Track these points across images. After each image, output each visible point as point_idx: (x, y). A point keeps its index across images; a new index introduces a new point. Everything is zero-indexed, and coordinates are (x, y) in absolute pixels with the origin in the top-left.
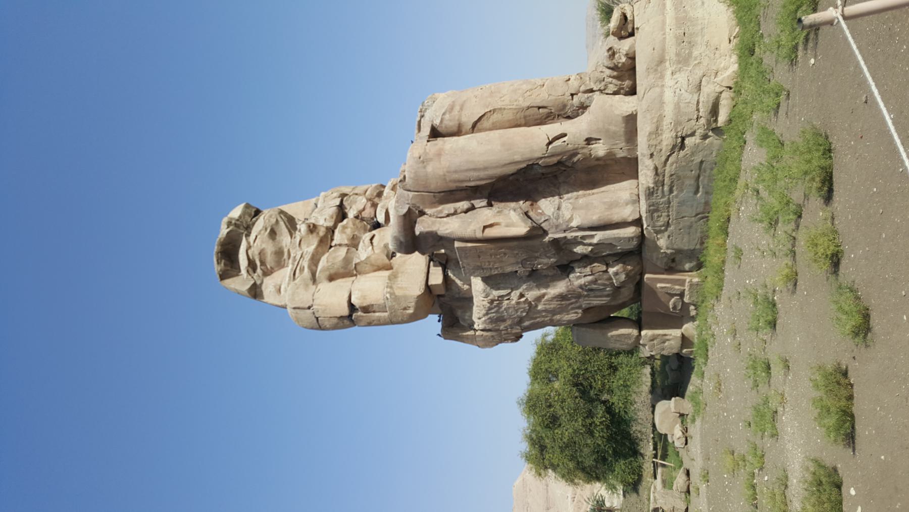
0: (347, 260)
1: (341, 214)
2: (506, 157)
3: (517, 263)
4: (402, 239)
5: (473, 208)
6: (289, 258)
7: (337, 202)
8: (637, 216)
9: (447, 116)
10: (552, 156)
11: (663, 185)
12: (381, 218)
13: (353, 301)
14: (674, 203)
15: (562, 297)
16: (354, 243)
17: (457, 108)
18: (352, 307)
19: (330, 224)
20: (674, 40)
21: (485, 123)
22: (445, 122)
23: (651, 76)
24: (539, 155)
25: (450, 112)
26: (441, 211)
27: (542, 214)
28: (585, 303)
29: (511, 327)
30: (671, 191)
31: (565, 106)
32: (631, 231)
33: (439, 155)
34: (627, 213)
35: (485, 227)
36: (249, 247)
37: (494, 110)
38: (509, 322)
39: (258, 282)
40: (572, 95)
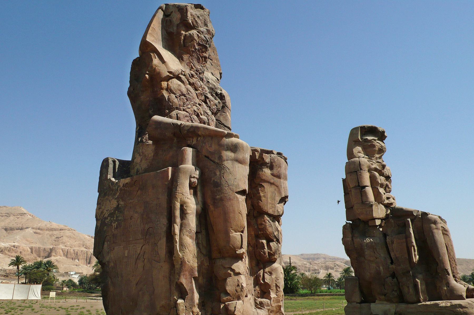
2: (441, 254)
16: (382, 186)
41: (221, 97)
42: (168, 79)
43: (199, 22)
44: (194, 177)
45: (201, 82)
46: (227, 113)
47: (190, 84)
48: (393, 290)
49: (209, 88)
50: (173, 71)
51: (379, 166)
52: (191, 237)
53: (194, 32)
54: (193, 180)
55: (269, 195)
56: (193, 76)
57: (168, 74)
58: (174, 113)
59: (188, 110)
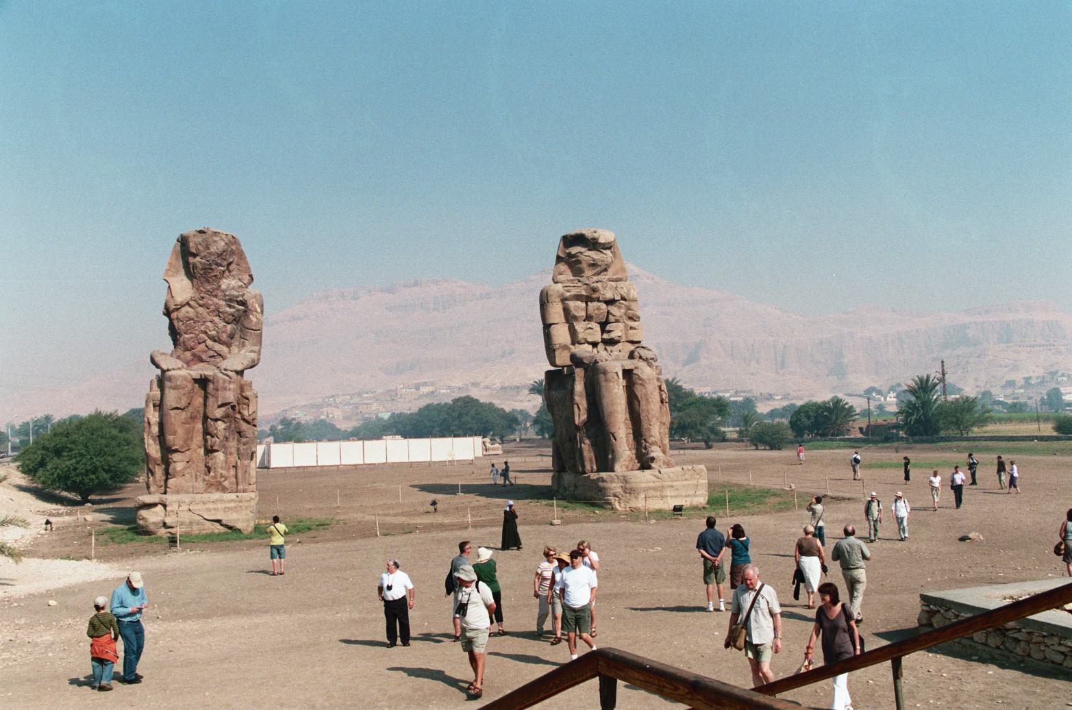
0: (576, 318)
1: (610, 302)
2: (606, 413)
9: (637, 376)
12: (608, 328)
13: (553, 326)
17: (640, 382)
18: (551, 325)
19: (601, 299)
23: (622, 478)
25: (638, 378)
32: (580, 468)
34: (588, 467)
35: (577, 404)
36: (581, 253)
37: (639, 402)
41: (243, 303)
42: (173, 311)
43: (201, 248)
45: (215, 300)
46: (251, 316)
47: (200, 306)
49: (225, 301)
50: (179, 303)
51: (586, 290)
52: (154, 440)
53: (198, 259)
54: (155, 402)
55: (211, 403)
56: (203, 298)
58: (181, 339)
59: (194, 332)
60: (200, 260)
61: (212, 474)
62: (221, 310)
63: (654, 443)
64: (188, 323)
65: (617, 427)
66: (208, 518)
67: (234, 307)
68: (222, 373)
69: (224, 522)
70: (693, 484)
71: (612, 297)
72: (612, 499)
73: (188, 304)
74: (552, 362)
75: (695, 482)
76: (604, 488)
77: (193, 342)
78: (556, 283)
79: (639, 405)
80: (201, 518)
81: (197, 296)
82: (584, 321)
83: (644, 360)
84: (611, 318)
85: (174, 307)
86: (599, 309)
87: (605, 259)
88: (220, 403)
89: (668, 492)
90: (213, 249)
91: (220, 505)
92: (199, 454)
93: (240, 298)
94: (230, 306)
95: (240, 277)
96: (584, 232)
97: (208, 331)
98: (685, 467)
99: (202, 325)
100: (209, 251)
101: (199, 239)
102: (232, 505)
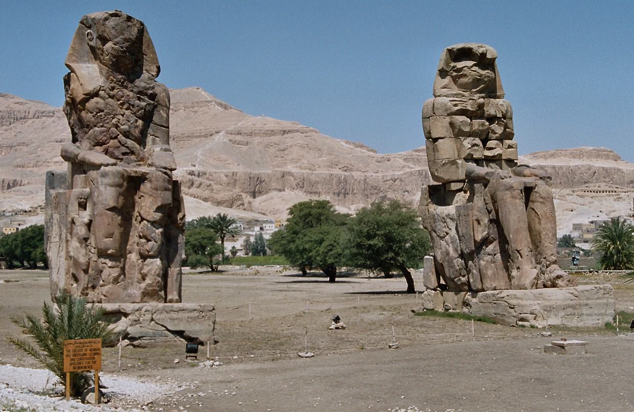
3: (463, 234)
4: (472, 175)
5: (489, 212)
6: (463, 91)
7: (499, 115)
8: (485, 290)
10: (512, 252)
11: (497, 300)
12: (491, 144)
14: (490, 305)
15: (448, 254)
17: (541, 200)
20: (551, 304)
21: (533, 214)
22: (535, 193)
24: (513, 245)
26: (487, 196)
27: (487, 247)
28: (445, 264)
29: (431, 226)
30: (495, 303)
31: (541, 254)
33: (514, 197)
34: (487, 284)
36: (470, 68)
37: (540, 219)
38: (434, 225)
39: (449, 74)
40: (545, 258)
41: (153, 97)
44: (81, 198)
45: (125, 91)
46: (161, 112)
48: (460, 275)
53: (109, 45)
54: (82, 200)
57: (83, 96)
59: (105, 125)
60: (113, 46)
61: (148, 281)
62: (132, 103)
63: (555, 262)
64: (98, 114)
65: (523, 246)
66: (169, 328)
67: (144, 100)
68: (161, 171)
69: (187, 333)
70: (605, 304)
71: (495, 114)
72: (530, 317)
73: (96, 94)
74: (435, 178)
75: (604, 301)
76: (519, 306)
77: (105, 136)
78: (436, 96)
79: (540, 223)
80: (164, 328)
81: (108, 85)
82: (469, 136)
83: (541, 178)
84: (491, 135)
85: (83, 96)
86: (483, 125)
87: (491, 75)
88: (159, 204)
89: (585, 311)
90: (127, 35)
91: (181, 315)
92: (130, 259)
93: (151, 92)
94: (139, 99)
95: (148, 68)
96: (471, 46)
97: (119, 125)
98: (596, 286)
99: (113, 118)
100: (123, 37)
101: (112, 22)
102: (196, 314)
